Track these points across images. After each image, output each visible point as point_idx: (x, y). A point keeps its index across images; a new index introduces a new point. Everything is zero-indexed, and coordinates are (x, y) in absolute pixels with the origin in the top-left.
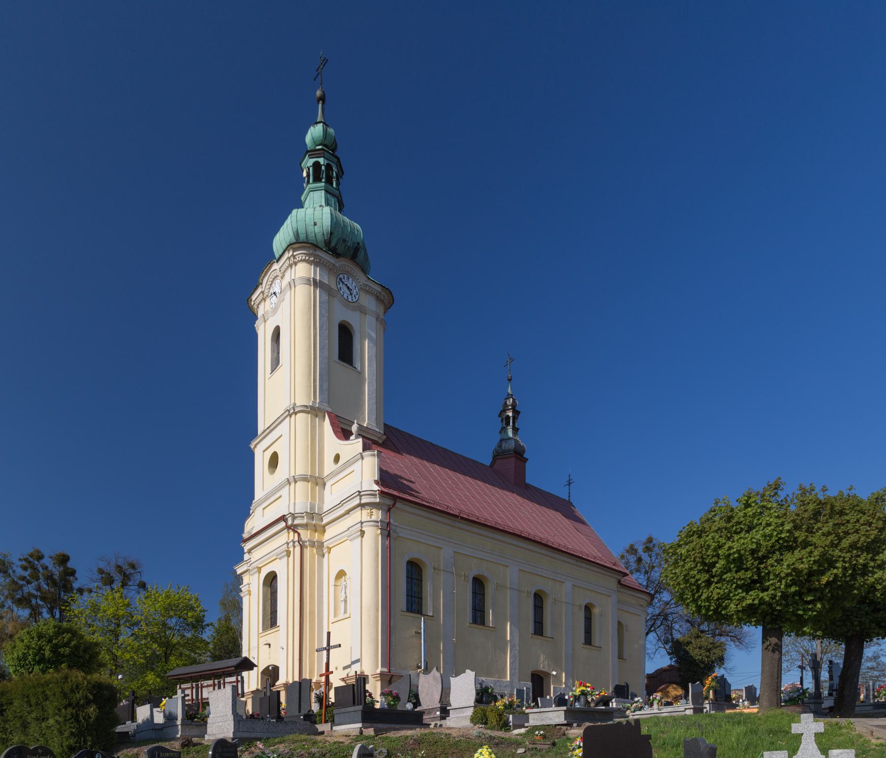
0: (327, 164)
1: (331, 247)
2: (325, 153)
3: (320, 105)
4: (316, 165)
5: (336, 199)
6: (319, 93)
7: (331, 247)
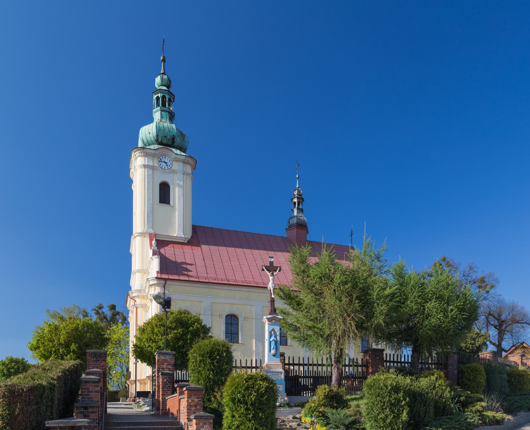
0: (162, 96)
1: (159, 142)
2: (161, 91)
3: (163, 64)
4: (158, 98)
5: (167, 113)
6: (162, 58)
7: (159, 142)
